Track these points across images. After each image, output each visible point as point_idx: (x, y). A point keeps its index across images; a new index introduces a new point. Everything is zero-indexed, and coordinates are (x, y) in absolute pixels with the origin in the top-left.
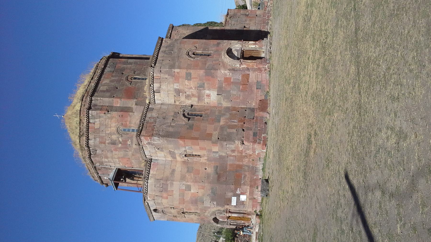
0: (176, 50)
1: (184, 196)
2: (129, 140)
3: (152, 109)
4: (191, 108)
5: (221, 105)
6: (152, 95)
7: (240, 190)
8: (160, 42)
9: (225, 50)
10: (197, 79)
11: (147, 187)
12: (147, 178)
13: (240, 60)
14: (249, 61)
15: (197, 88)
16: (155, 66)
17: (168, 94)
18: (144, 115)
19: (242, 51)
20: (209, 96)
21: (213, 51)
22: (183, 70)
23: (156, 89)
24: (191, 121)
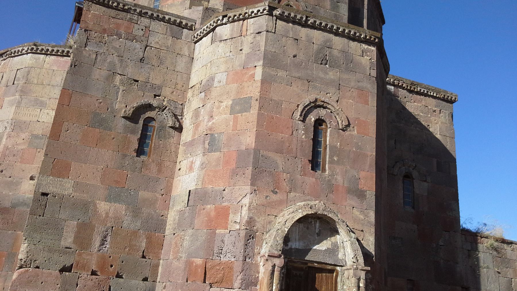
0: (332, 75)
3: (177, 37)
4: (170, 123)
5: (172, 206)
6: (207, 27)
8: (362, 37)
9: (331, 211)
10: (233, 131)
11: (20, 53)
12: (35, 49)
13: (279, 257)
14: (274, 288)
15: (209, 132)
16: (275, 18)
17: (206, 65)
18: (158, 16)
19: (330, 267)
20: (191, 169)
21: (332, 175)
22: (259, 89)
24: (126, 127)
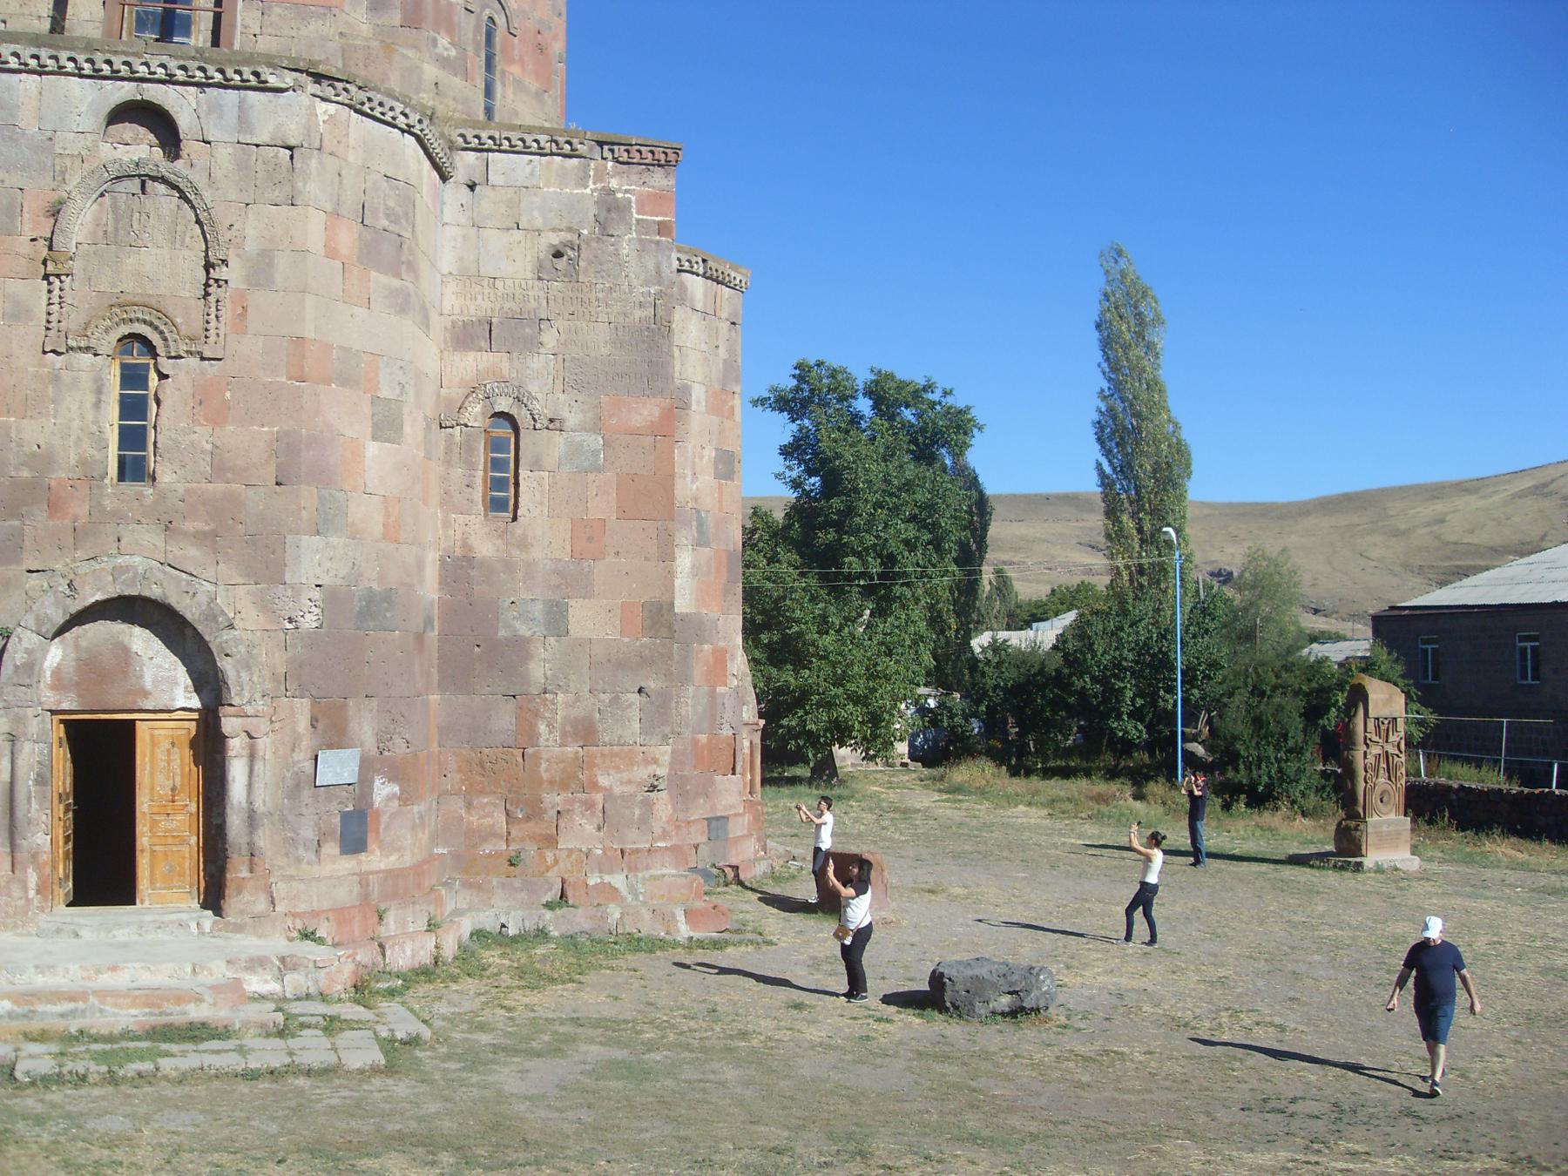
1: (346, 381)
2: (453, 53)
7: (389, 798)
11: (388, 118)
23: (689, 285)
